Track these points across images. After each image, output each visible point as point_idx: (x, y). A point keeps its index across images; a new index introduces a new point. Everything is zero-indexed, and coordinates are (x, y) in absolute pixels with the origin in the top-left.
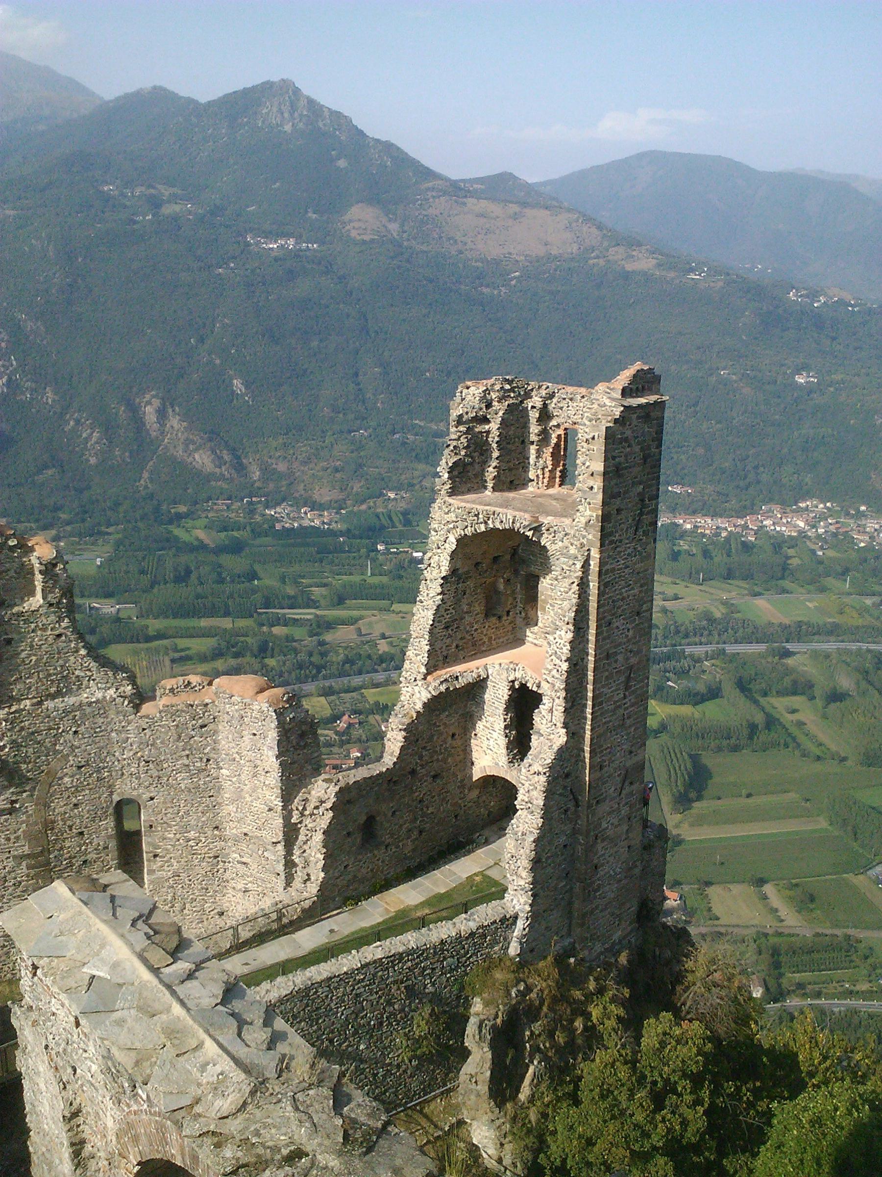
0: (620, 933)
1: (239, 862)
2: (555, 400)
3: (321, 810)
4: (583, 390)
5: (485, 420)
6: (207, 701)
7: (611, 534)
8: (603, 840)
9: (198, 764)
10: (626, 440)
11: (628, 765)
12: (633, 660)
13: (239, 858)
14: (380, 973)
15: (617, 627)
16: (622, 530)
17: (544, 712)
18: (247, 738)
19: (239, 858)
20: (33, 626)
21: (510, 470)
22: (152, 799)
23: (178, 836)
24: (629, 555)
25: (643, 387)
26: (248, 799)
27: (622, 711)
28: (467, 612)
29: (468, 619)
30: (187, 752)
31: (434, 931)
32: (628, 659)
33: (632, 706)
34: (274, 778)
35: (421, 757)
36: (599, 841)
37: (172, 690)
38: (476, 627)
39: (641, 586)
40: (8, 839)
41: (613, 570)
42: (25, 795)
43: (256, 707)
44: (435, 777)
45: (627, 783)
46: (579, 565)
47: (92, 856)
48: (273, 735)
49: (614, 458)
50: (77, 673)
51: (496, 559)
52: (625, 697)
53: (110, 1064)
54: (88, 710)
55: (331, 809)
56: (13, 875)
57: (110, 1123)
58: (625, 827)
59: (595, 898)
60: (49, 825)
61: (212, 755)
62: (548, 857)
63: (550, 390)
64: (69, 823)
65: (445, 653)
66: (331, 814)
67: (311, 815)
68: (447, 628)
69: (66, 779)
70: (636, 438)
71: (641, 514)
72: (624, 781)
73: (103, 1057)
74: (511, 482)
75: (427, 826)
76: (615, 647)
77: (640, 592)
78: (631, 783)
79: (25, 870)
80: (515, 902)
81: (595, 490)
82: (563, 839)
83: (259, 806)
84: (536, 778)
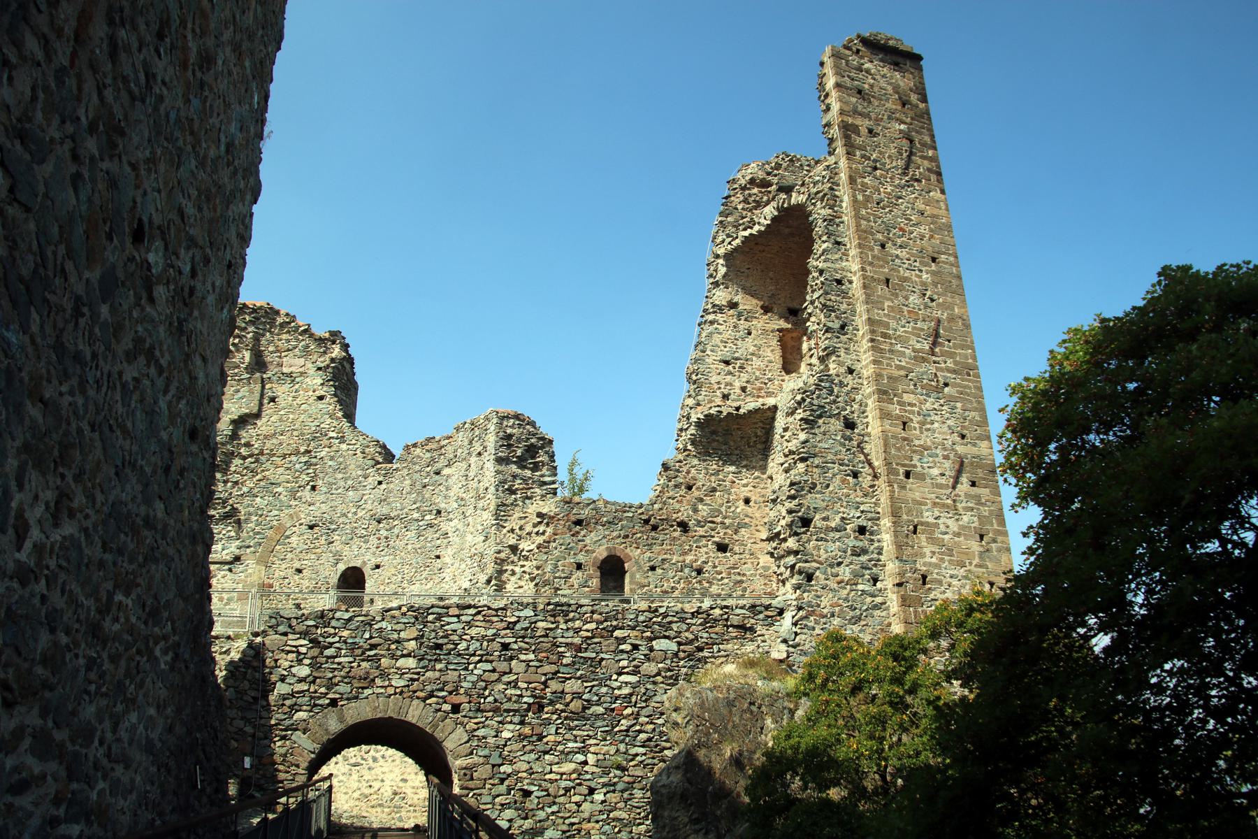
10: (868, 71)
11: (960, 449)
15: (897, 256)
28: (753, 354)
29: (756, 362)
36: (923, 537)
39: (931, 230)
42: (248, 550)
45: (964, 479)
48: (491, 440)
54: (330, 463)
61: (442, 506)
68: (727, 363)
69: (294, 539)
72: (959, 472)
77: (931, 237)
78: (973, 484)
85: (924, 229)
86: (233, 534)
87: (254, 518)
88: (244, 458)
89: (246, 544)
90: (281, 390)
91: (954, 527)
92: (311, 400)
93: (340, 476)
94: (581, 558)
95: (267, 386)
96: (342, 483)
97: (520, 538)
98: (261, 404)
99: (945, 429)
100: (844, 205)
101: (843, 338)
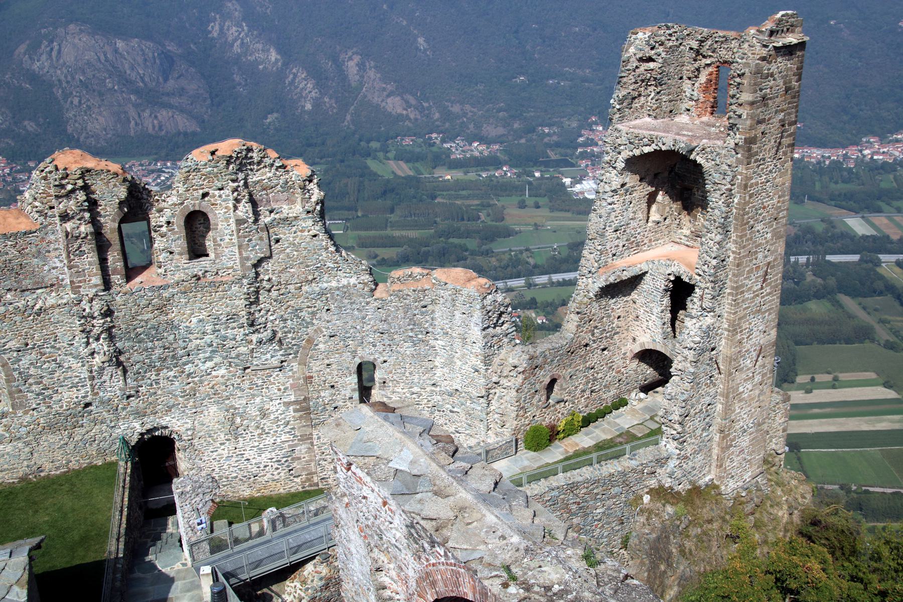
0: (750, 474)
1: (451, 411)
2: (709, 42)
3: (514, 373)
4: (731, 34)
5: (650, 59)
6: (427, 287)
7: (757, 154)
8: (740, 401)
9: (420, 336)
10: (772, 75)
11: (761, 342)
12: (770, 259)
13: (451, 408)
14: (562, 497)
15: (758, 231)
16: (765, 150)
17: (695, 300)
18: (458, 314)
19: (451, 408)
20: (294, 229)
21: (670, 101)
22: (385, 362)
23: (405, 391)
24: (771, 171)
25: (788, 29)
26: (459, 363)
27: (759, 299)
29: (633, 224)
30: (411, 327)
31: (604, 468)
32: (766, 257)
33: (767, 295)
34: (478, 348)
35: (593, 335)
37: (399, 279)
38: (639, 230)
39: (779, 197)
40: (279, 390)
41: (757, 184)
42: (290, 357)
43: (465, 292)
44: (603, 350)
46: (728, 179)
47: (340, 403)
48: (477, 316)
49: (761, 90)
50: (329, 264)
51: (656, 175)
52: (762, 288)
53: (413, 531)
54: (337, 292)
55: (523, 372)
56: (283, 416)
57: (411, 573)
58: (757, 392)
59: (731, 446)
60: (309, 379)
61: (430, 330)
62: (696, 414)
63: (705, 34)
64: (323, 379)
65: (614, 252)
66: (521, 377)
67: (507, 376)
69: (321, 346)
70: (780, 73)
71: (782, 137)
72: (758, 356)
73: (407, 526)
74: (671, 111)
75: (597, 388)
76: (756, 247)
77: (778, 202)
79: (292, 413)
80: (668, 446)
81: (744, 116)
82: (708, 399)
83: (467, 368)
84: (686, 352)
85: (775, 201)
86: (277, 348)
87: (290, 335)
88: (269, 291)
89: (289, 351)
90: (284, 233)
91: (750, 387)
92: (308, 240)
93: (347, 301)
94: (538, 387)
95: (271, 231)
96: (349, 306)
97: (500, 377)
98: (270, 246)
99: (758, 333)
100: (736, 200)
101: (719, 298)
